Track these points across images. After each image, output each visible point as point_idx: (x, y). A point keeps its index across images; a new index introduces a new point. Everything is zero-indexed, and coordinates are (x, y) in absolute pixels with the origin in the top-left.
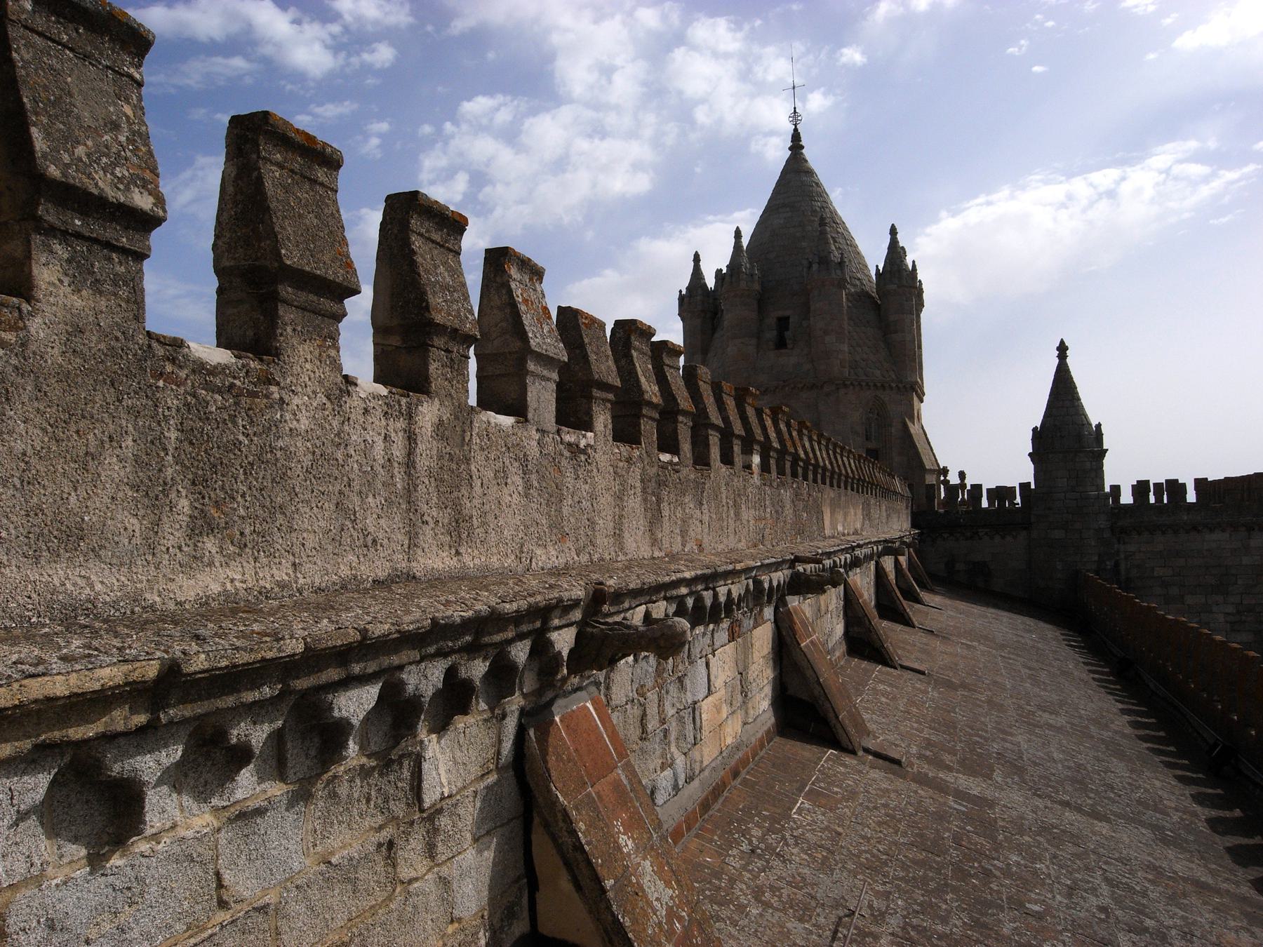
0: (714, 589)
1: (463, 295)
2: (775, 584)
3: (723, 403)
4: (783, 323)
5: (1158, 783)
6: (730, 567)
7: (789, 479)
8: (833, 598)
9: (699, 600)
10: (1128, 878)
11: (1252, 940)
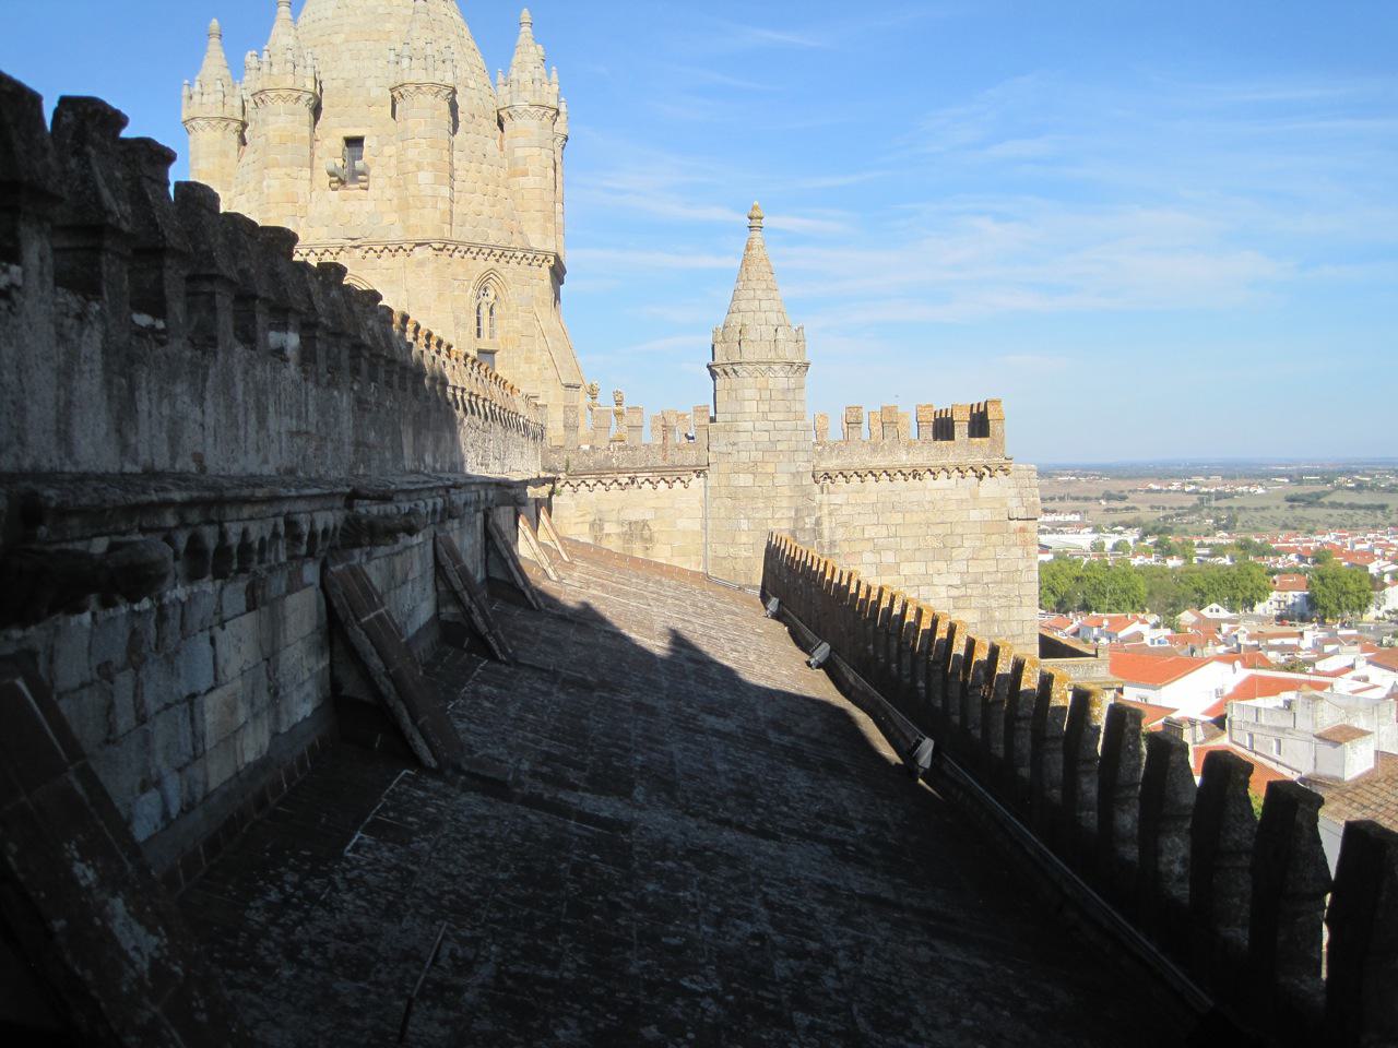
0: (221, 524)
2: (320, 527)
5: (844, 792)
6: (246, 492)
9: (195, 542)
10: (793, 900)
11: (931, 953)
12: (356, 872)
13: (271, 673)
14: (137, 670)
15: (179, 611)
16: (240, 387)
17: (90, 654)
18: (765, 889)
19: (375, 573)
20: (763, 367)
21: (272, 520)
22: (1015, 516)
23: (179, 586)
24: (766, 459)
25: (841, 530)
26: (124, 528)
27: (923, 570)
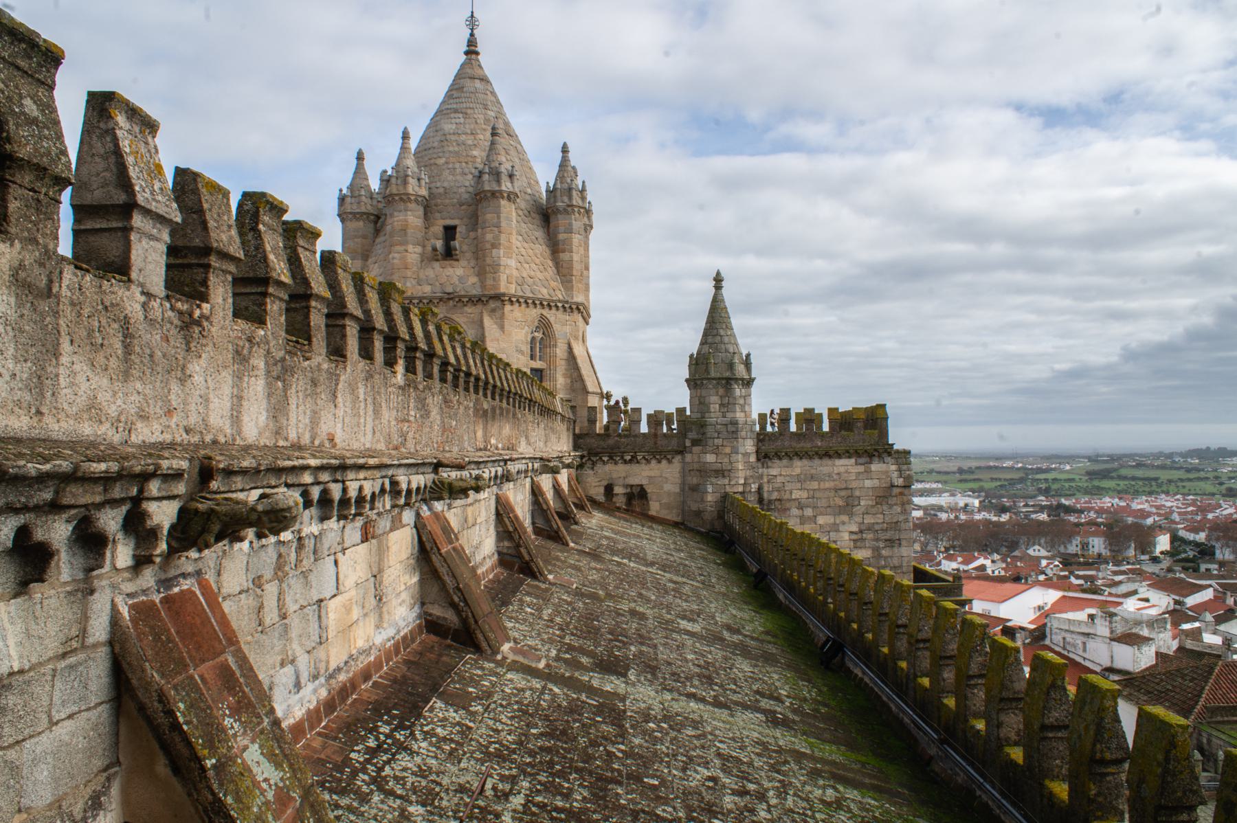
0: (343, 482)
1: (56, 134)
3: (365, 295)
4: (450, 232)
5: (776, 676)
6: (361, 461)
7: (437, 384)
8: (482, 507)
9: (325, 493)
12: (430, 727)
14: (281, 581)
15: (313, 541)
16: (361, 391)
17: (247, 570)
18: (718, 744)
19: (454, 521)
20: (724, 382)
21: (380, 481)
26: (274, 484)
27: (832, 521)
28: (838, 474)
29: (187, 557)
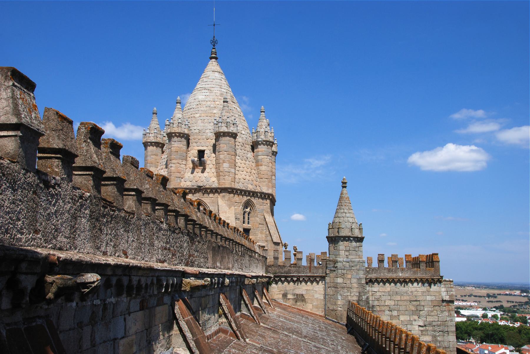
4: (201, 153)
13: (148, 334)
15: (112, 306)
17: (74, 318)
21: (151, 278)
22: (445, 299)
23: (112, 297)
24: (348, 273)
25: (377, 302)
27: (408, 319)
28: (412, 292)
29: (41, 307)
